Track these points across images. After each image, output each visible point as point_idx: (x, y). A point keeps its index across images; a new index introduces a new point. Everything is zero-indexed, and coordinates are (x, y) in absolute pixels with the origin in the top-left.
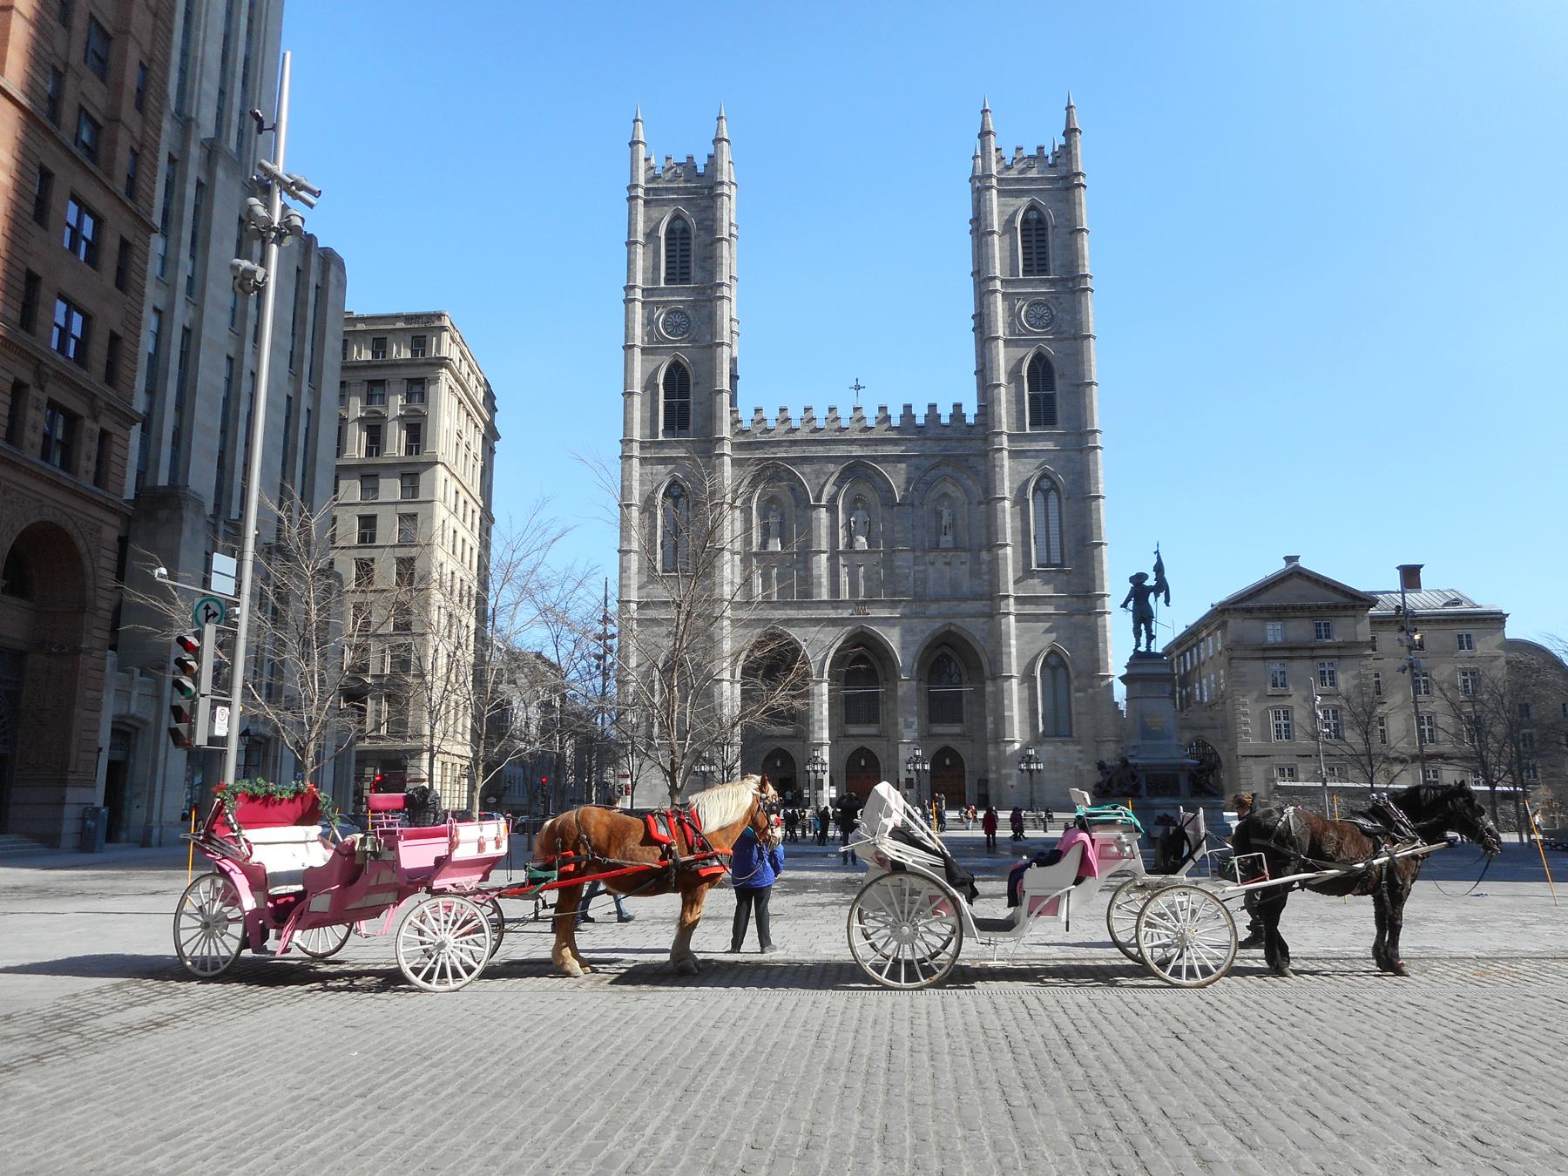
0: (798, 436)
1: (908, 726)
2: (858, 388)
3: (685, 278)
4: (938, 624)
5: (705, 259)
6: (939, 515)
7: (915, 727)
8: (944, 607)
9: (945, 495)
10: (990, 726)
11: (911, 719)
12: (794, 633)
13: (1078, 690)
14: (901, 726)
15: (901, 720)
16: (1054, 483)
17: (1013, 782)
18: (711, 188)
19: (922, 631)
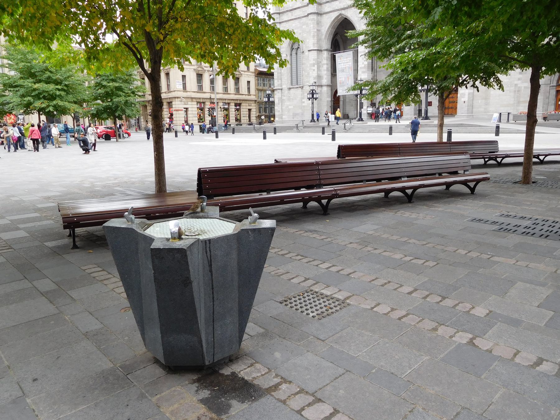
17: (466, 99)
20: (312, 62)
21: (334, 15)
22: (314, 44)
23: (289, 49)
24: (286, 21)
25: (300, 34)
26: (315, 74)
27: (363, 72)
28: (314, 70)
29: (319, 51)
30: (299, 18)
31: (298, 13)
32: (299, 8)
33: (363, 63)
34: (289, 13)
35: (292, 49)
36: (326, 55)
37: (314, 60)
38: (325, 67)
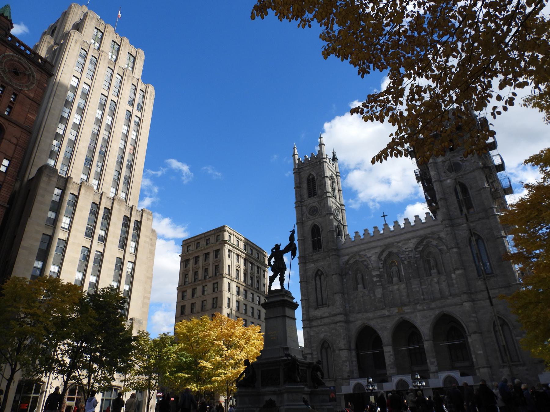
2: (384, 216)
3: (315, 194)
4: (437, 312)
6: (429, 261)
7: (436, 363)
10: (474, 360)
11: (432, 360)
12: (372, 323)
14: (429, 364)
15: (428, 361)
16: (479, 236)
18: (320, 161)
20: (344, 359)
21: (359, 323)
24: (315, 326)
25: (330, 336)
26: (348, 369)
28: (347, 366)
29: (349, 349)
31: (326, 321)
32: (328, 317)
33: (390, 361)
35: (322, 347)
36: (354, 353)
38: (355, 363)
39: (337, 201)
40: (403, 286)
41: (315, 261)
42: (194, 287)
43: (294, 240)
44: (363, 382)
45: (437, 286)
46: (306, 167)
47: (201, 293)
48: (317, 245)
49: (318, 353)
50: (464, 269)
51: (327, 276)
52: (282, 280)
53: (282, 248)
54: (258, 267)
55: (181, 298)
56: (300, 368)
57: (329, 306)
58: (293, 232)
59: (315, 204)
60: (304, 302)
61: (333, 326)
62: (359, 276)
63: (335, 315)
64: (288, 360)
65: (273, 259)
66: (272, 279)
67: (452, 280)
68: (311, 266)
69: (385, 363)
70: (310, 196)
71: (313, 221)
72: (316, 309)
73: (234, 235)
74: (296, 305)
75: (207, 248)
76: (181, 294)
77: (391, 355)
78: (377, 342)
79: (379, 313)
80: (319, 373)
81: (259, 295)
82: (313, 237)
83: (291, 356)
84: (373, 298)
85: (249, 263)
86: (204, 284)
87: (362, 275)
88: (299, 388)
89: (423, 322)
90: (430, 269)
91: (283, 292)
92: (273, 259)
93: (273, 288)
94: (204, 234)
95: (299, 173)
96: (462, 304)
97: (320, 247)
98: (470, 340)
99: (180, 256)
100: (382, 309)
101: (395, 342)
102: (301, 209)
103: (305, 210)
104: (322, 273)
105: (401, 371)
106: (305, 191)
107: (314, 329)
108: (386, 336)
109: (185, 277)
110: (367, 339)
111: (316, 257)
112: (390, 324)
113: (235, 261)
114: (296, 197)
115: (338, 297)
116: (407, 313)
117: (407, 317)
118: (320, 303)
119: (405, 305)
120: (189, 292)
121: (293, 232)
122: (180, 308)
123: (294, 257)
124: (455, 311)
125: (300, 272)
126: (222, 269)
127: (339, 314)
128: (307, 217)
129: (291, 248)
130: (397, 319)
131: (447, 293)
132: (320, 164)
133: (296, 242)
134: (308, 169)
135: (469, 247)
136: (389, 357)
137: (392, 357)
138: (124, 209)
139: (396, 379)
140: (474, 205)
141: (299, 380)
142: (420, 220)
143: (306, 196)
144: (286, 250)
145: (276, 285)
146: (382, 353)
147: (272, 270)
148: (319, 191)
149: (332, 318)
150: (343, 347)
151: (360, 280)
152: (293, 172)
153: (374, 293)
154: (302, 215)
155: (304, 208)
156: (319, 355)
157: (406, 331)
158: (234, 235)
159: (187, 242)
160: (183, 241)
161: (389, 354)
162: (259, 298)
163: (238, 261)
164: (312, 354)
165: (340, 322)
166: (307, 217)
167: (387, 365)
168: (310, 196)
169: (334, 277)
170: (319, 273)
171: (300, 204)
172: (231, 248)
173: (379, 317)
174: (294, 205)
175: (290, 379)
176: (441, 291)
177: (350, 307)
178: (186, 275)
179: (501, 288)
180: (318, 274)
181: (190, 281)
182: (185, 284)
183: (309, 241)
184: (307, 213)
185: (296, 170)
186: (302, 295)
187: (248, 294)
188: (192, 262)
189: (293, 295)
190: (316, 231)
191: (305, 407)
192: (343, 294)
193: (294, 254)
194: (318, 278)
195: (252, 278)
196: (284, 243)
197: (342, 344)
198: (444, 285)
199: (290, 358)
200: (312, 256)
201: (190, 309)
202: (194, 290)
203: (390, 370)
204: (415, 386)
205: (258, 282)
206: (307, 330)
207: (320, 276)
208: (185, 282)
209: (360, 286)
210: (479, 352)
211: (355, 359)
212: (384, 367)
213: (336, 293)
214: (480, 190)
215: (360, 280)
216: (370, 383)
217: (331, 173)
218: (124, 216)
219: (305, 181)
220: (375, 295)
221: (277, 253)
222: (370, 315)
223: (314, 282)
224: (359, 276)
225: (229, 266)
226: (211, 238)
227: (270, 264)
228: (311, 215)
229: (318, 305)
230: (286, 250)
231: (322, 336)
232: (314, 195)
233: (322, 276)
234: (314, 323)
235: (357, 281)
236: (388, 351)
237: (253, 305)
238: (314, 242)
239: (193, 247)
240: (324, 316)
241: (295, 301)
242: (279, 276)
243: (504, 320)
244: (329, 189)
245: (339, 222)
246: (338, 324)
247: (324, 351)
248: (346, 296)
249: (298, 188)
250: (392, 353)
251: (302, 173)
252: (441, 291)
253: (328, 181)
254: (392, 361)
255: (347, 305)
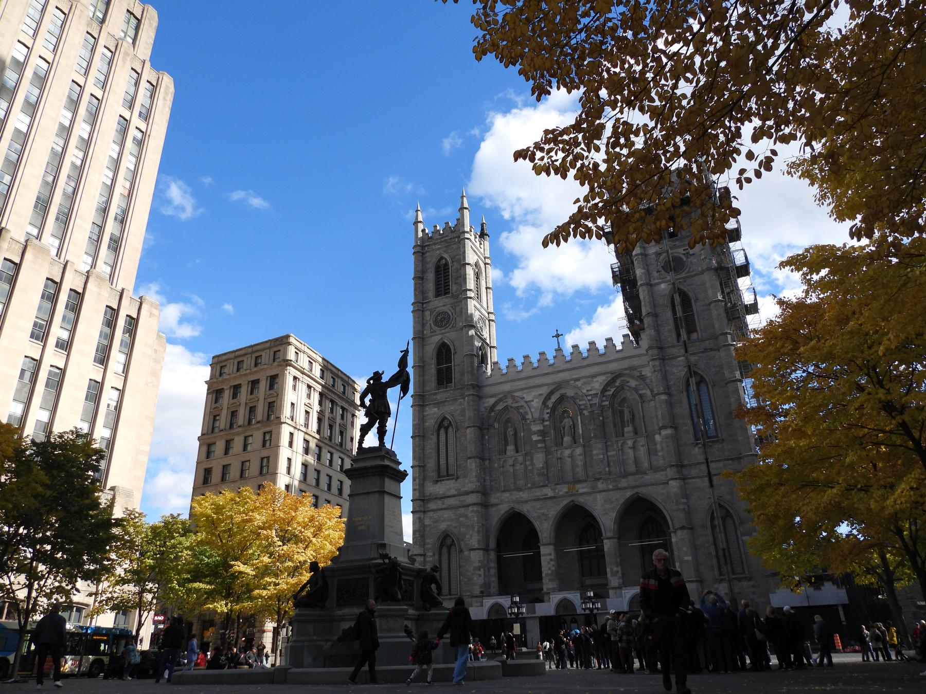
0: (523, 375)
1: (614, 574)
2: (557, 336)
3: (447, 292)
4: (628, 494)
5: (457, 278)
6: (622, 412)
7: (620, 574)
8: (631, 480)
9: (625, 399)
11: (615, 569)
12: (525, 509)
13: (744, 534)
14: (609, 575)
15: (608, 570)
16: (702, 377)
19: (617, 500)
20: (477, 564)
21: (504, 508)
22: (479, 542)
23: (437, 546)
24: (433, 510)
25: (455, 527)
26: (481, 581)
27: (550, 580)
28: (480, 575)
29: (486, 550)
30: (454, 508)
32: (454, 496)
34: (440, 502)
35: (442, 545)
36: (493, 556)
37: (480, 561)
38: (494, 571)
39: (482, 306)
40: (579, 451)
41: (439, 404)
42: (229, 438)
43: (406, 366)
44: (505, 601)
45: (631, 452)
46: (435, 244)
47: (241, 448)
48: (444, 377)
49: (434, 554)
50: (675, 428)
51: (457, 430)
52: (382, 433)
53: (385, 379)
54: (343, 409)
55: (204, 455)
56: (403, 577)
57: (458, 478)
58: (406, 352)
59: (445, 309)
60: (417, 469)
61: (462, 510)
62: (510, 431)
63: (467, 493)
64: (384, 563)
65: (369, 397)
66: (365, 430)
67: (655, 444)
68: (433, 412)
69: (540, 572)
70: (438, 294)
71: (440, 337)
72: (436, 482)
73: (304, 352)
74: (403, 475)
75: (256, 372)
76: (205, 448)
77: (551, 560)
78: (531, 538)
79: (538, 493)
80: (433, 586)
81: (342, 456)
82: (439, 363)
83: (389, 558)
84: (530, 468)
85: (327, 402)
86: (247, 434)
87: (515, 430)
88: (399, 610)
89: (605, 509)
90: (623, 426)
91: (381, 452)
92: (369, 397)
93: (366, 445)
94: (252, 346)
95: (423, 254)
96: (668, 483)
97: (449, 380)
98: (674, 540)
99: (206, 382)
100: (543, 486)
101: (559, 541)
102: (423, 314)
103: (428, 318)
104: (450, 424)
105: (564, 585)
106: (430, 286)
107: (431, 514)
108: (545, 529)
109: (215, 420)
110: (515, 532)
111: (442, 396)
112: (553, 511)
113: (304, 395)
114: (415, 295)
115: (472, 464)
116: (582, 494)
117: (581, 500)
118: (443, 472)
119: (579, 482)
120: (220, 446)
121: (406, 352)
122: (202, 473)
123: (405, 394)
124: (656, 494)
125: (413, 420)
126: (281, 407)
127: (473, 492)
128: (431, 328)
129: (400, 379)
130: (565, 502)
131: (646, 464)
132: (459, 242)
133: (410, 370)
134: (438, 249)
135: (685, 393)
136: (549, 563)
137: (553, 563)
138: (107, 295)
139: (556, 598)
140: (698, 327)
141: (400, 597)
142: (614, 345)
143: (431, 294)
144: (392, 382)
145: (371, 440)
146: (538, 555)
147: (366, 415)
148: (453, 288)
149: (461, 498)
150: (477, 546)
151: (510, 439)
152: (413, 251)
153: (532, 460)
154: (423, 325)
155: (427, 313)
156: (437, 557)
157: (577, 522)
158: (304, 352)
159: (220, 359)
160: (214, 358)
161: (549, 557)
162: (342, 460)
163: (309, 396)
164: (424, 555)
165: (474, 504)
166: (431, 328)
167: (544, 575)
168: (438, 294)
169: (468, 430)
170: (446, 424)
171: (420, 306)
172: (299, 375)
173: (538, 499)
174: (411, 308)
175: (386, 595)
176: (637, 461)
177: (491, 481)
178: (215, 417)
179: (728, 460)
180: (443, 424)
181: (222, 427)
182: (212, 432)
183: (432, 370)
184: (431, 322)
185: (418, 249)
186: (414, 458)
187: (323, 454)
188: (227, 394)
189: (399, 458)
190: (444, 353)
191: (408, 640)
192: (482, 459)
193: (405, 390)
194: (442, 431)
195: (331, 427)
196: (389, 371)
197: (473, 539)
198: (642, 451)
199: (387, 561)
200: (434, 394)
201: (220, 475)
202: (228, 443)
203: (548, 584)
204: (584, 610)
205: (341, 433)
206: (418, 515)
207: (446, 429)
208: (213, 428)
209: (511, 448)
210: (686, 558)
211: (493, 565)
212: (540, 578)
213: (470, 458)
214: (709, 304)
215: (510, 439)
216: (516, 603)
217: (476, 257)
218: (71, 290)
219: (431, 267)
220: (532, 464)
221: (377, 387)
222: (524, 495)
223: (434, 438)
224: (510, 431)
225: (293, 404)
226: (263, 354)
227: (363, 404)
228: (438, 326)
229: (439, 477)
230: (392, 382)
231: (443, 526)
232: (445, 294)
233: (450, 430)
234: (432, 506)
235: (506, 440)
236: (547, 553)
237: (331, 472)
238: (439, 372)
239: (230, 368)
240: (448, 494)
241: (402, 468)
242: (377, 425)
243: (728, 511)
244: (471, 284)
245: (484, 340)
246: (471, 508)
247: (445, 550)
248: (487, 462)
249: (419, 278)
250: (552, 557)
251: (428, 254)
252: (637, 461)
253: (470, 272)
254: (553, 568)
255: (488, 478)
